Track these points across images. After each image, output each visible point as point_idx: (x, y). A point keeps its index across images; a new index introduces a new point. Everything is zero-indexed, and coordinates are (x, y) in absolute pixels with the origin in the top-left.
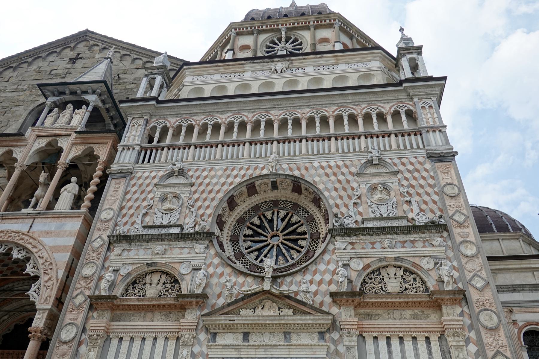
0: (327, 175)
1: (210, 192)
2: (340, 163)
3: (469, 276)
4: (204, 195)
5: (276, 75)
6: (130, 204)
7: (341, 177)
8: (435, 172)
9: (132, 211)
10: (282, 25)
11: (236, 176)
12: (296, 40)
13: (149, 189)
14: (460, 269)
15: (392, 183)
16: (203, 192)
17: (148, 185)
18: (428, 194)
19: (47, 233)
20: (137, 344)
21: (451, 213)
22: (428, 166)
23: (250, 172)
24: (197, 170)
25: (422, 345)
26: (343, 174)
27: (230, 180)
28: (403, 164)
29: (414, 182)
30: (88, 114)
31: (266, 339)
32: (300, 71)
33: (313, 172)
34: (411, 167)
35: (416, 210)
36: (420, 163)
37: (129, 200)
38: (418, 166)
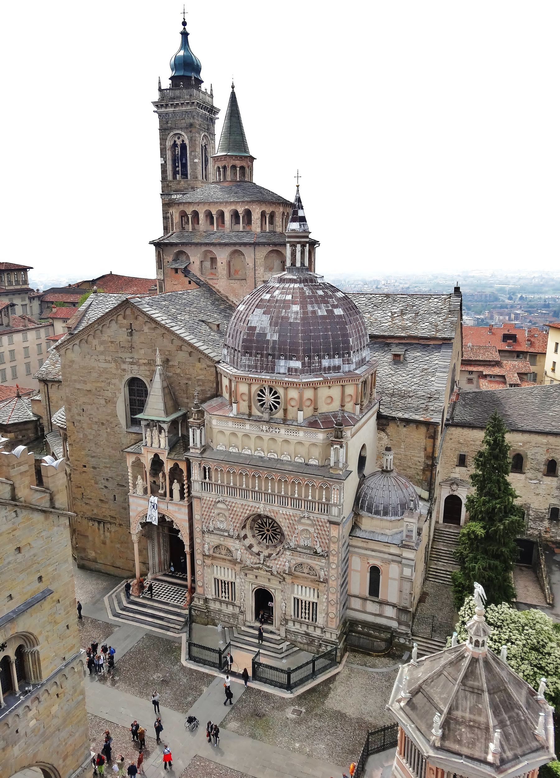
0: (285, 518)
1: (237, 515)
2: (291, 514)
3: (331, 575)
4: (235, 517)
5: (262, 433)
6: (205, 513)
7: (291, 522)
8: (330, 529)
9: (207, 517)
10: (265, 381)
11: (247, 510)
12: (275, 393)
13: (211, 507)
14: (328, 572)
15: (311, 530)
16: (234, 515)
17: (211, 505)
18: (325, 539)
19: (176, 512)
20: (222, 569)
21: (331, 549)
22: (328, 525)
23: (253, 509)
24: (230, 502)
25: (312, 590)
26: (292, 520)
27: (244, 511)
28: (318, 521)
29: (320, 532)
30: (167, 438)
31: (263, 579)
32: (277, 430)
33: (279, 515)
34: (321, 524)
35: (318, 546)
36: (325, 522)
37: (204, 511)
38: (324, 524)
